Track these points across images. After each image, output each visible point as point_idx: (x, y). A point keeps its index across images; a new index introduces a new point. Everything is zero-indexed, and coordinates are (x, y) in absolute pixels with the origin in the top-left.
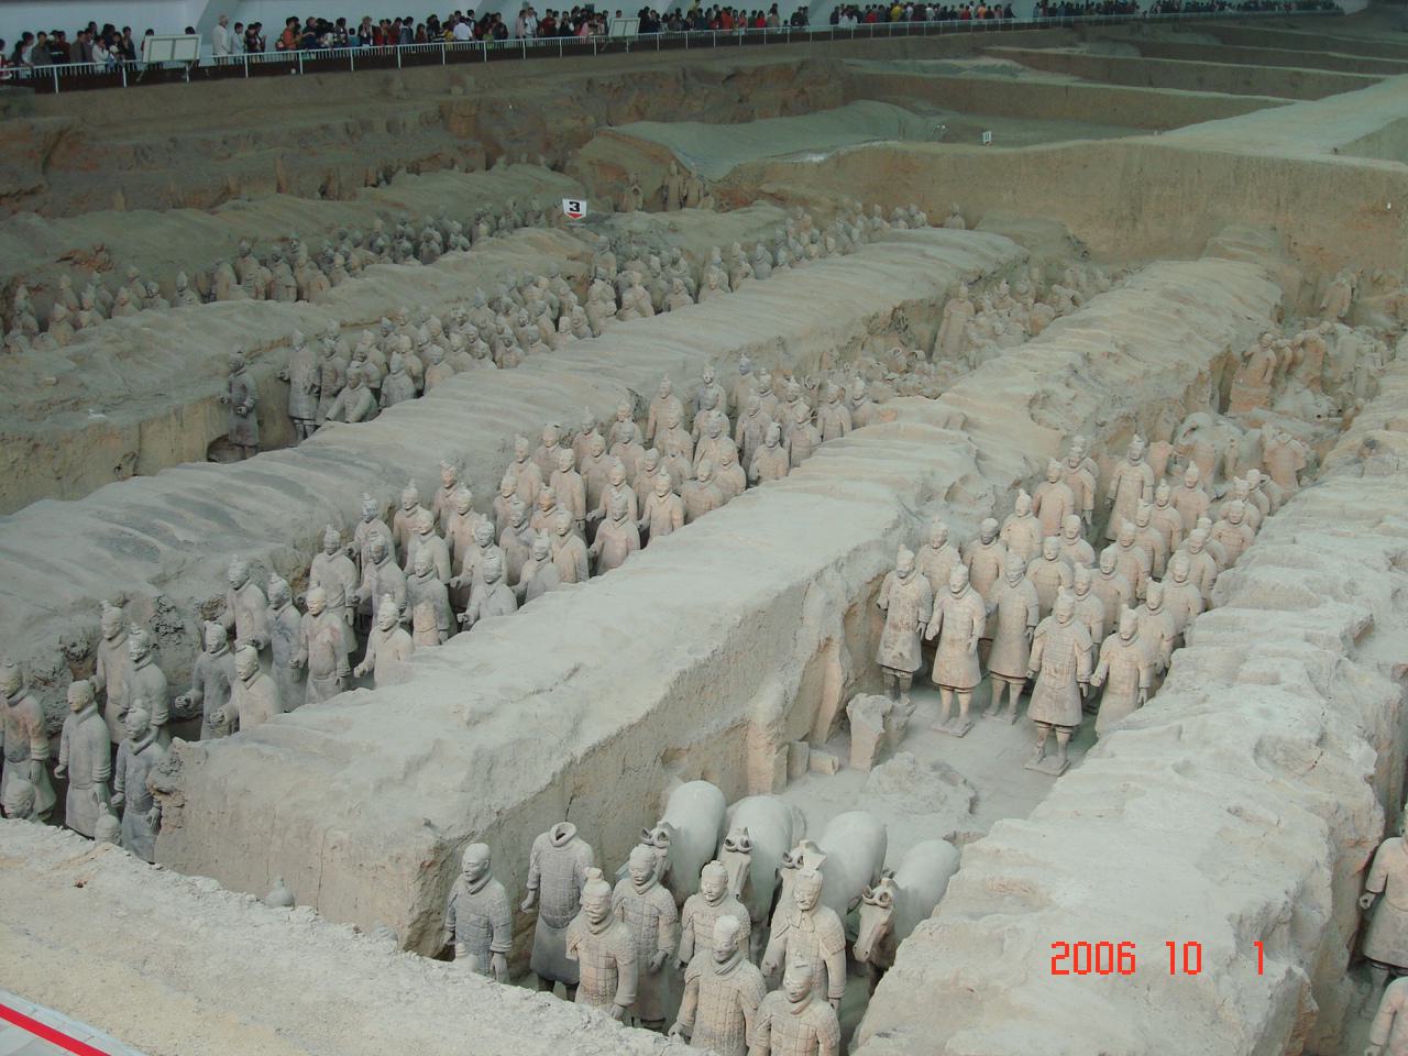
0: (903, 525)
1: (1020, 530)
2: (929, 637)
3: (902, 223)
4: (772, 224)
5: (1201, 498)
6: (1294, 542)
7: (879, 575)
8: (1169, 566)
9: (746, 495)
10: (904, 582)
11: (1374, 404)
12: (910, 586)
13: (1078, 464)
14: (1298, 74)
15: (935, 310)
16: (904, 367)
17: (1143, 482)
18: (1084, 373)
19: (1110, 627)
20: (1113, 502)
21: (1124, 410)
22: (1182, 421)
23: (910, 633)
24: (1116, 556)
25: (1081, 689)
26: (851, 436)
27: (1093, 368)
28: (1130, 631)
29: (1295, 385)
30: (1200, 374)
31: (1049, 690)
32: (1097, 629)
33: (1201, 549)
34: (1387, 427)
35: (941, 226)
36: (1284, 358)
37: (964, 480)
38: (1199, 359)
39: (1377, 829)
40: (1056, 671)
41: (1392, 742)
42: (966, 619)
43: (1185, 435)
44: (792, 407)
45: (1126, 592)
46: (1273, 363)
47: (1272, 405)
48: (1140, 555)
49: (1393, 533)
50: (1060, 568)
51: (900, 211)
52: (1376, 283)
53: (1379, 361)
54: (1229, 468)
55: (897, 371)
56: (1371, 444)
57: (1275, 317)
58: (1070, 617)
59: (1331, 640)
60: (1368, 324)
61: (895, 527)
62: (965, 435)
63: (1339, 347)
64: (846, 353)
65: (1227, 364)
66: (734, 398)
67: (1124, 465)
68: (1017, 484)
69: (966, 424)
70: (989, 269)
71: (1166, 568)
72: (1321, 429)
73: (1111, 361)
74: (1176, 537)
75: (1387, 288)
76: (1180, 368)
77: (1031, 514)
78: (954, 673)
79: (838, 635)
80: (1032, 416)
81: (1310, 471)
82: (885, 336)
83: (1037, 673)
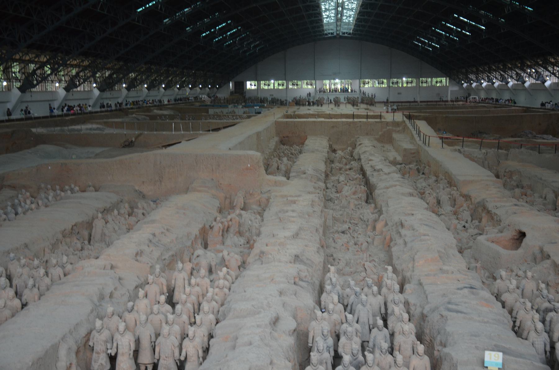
0: (94, 312)
1: (142, 304)
2: (113, 354)
3: (69, 192)
4: (12, 198)
5: (207, 280)
6: (245, 292)
7: (88, 333)
8: (201, 308)
9: (24, 311)
10: (99, 333)
11: (260, 238)
13: (159, 276)
14: (209, 122)
16: (80, 248)
17: (184, 279)
19: (184, 336)
20: (174, 289)
21: (171, 253)
22: (193, 254)
24: (182, 309)
25: (177, 363)
26: (64, 279)
28: (193, 336)
30: (196, 235)
32: (179, 337)
33: (211, 300)
34: (267, 245)
36: (225, 226)
37: (116, 289)
38: (195, 230)
40: (166, 357)
41: (294, 359)
42: (127, 344)
43: (195, 259)
44: (37, 271)
45: (187, 322)
46: (222, 228)
47: (223, 244)
48: (189, 306)
50: (161, 317)
51: (67, 187)
53: (258, 223)
54: (213, 269)
55: (77, 250)
56: (262, 253)
57: (219, 211)
58: (169, 334)
60: (251, 210)
61: (92, 311)
62: (112, 271)
63: (243, 219)
64: (54, 247)
65: (205, 231)
66: (8, 271)
67: (176, 273)
68: (137, 287)
70: (108, 206)
71: (199, 310)
72: (242, 250)
74: (201, 298)
75: (255, 196)
77: (145, 298)
78: (125, 367)
79: (74, 362)
81: (243, 265)
83: (158, 360)
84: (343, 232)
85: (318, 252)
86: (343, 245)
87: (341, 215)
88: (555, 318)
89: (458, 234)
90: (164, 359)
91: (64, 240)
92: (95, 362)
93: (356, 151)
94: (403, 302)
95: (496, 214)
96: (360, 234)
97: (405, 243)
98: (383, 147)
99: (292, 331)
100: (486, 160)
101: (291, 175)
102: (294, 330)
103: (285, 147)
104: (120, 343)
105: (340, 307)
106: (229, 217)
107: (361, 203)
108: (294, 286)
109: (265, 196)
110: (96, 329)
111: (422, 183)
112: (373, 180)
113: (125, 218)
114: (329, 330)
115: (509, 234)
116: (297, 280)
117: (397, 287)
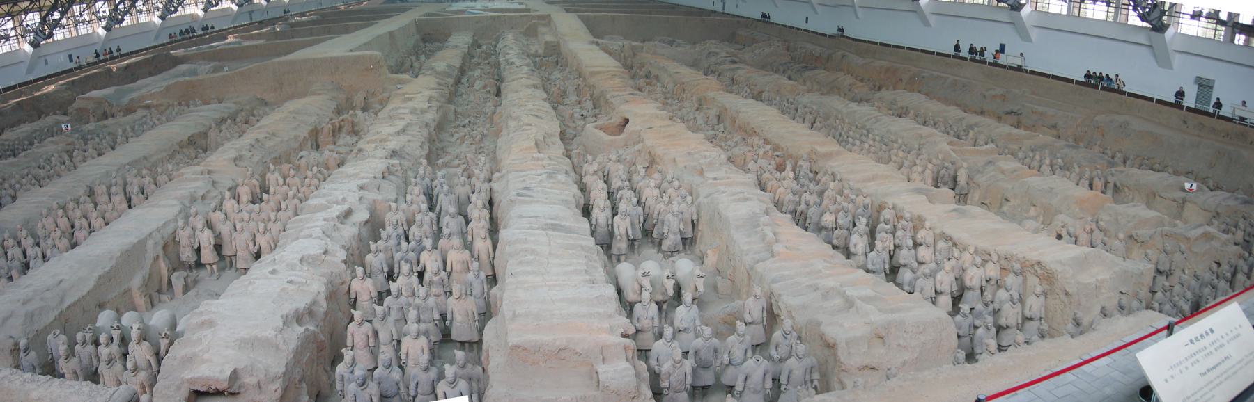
15: (205, 135)
18: (256, 146)
21: (273, 156)
27: (260, 144)
29: (343, 135)
30: (305, 137)
33: (293, 198)
36: (336, 126)
37: (208, 192)
38: (304, 132)
39: (349, 278)
41: (358, 248)
47: (335, 143)
49: (363, 178)
52: (374, 94)
56: (360, 150)
59: (333, 219)
61: (180, 212)
64: (171, 157)
69: (209, 172)
76: (296, 137)
80: (236, 165)
84: (464, 126)
85: (421, 147)
86: (458, 139)
87: (467, 109)
88: (624, 195)
89: (574, 122)
93: (498, 46)
94: (489, 189)
95: (612, 103)
96: (478, 127)
97: (509, 135)
98: (527, 40)
100: (622, 52)
101: (421, 72)
103: (427, 44)
105: (423, 197)
106: (341, 118)
107: (488, 96)
108: (382, 181)
109: (386, 95)
111: (556, 74)
112: (504, 74)
113: (238, 126)
114: (404, 219)
115: (616, 120)
116: (386, 174)
117: (482, 176)
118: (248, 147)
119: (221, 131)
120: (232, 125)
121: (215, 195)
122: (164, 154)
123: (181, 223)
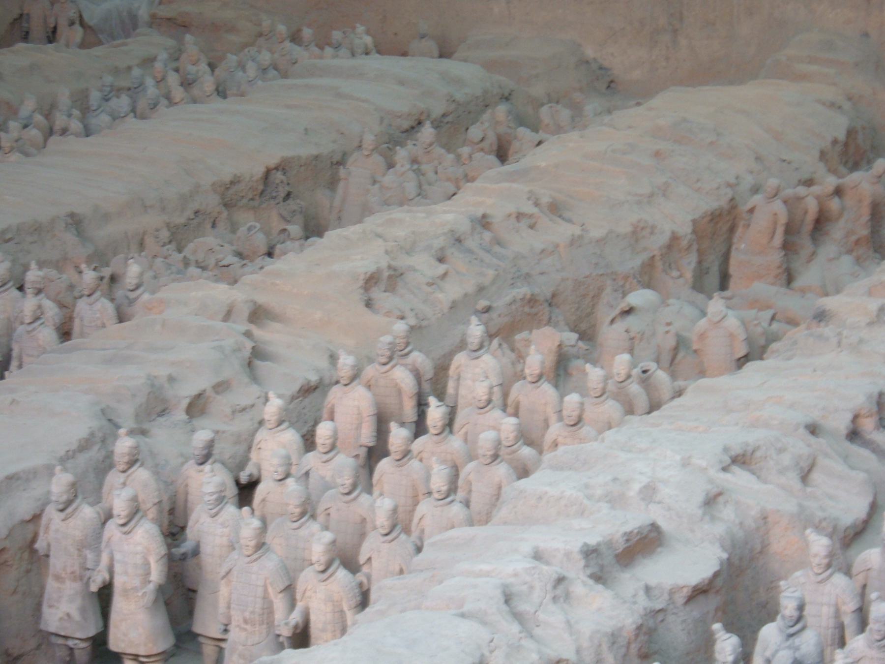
12: (72, 522)
18: (471, 243)
21: (523, 290)
23: (78, 586)
29: (829, 249)
30: (675, 238)
31: (240, 648)
35: (404, 54)
36: (806, 213)
37: (221, 387)
40: (246, 621)
42: (139, 560)
46: (783, 219)
61: (84, 446)
73: (523, 224)
80: (369, 304)
82: (254, 208)
90: (238, 626)
91: (225, 214)
92: (51, 606)
99: (686, 592)
102: (699, 592)
104: (118, 556)
110: (53, 498)
113: (459, 157)
118: (438, 243)
119: (391, 165)
120: (439, 151)
121: (244, 402)
122: (152, 220)
123: (60, 483)
